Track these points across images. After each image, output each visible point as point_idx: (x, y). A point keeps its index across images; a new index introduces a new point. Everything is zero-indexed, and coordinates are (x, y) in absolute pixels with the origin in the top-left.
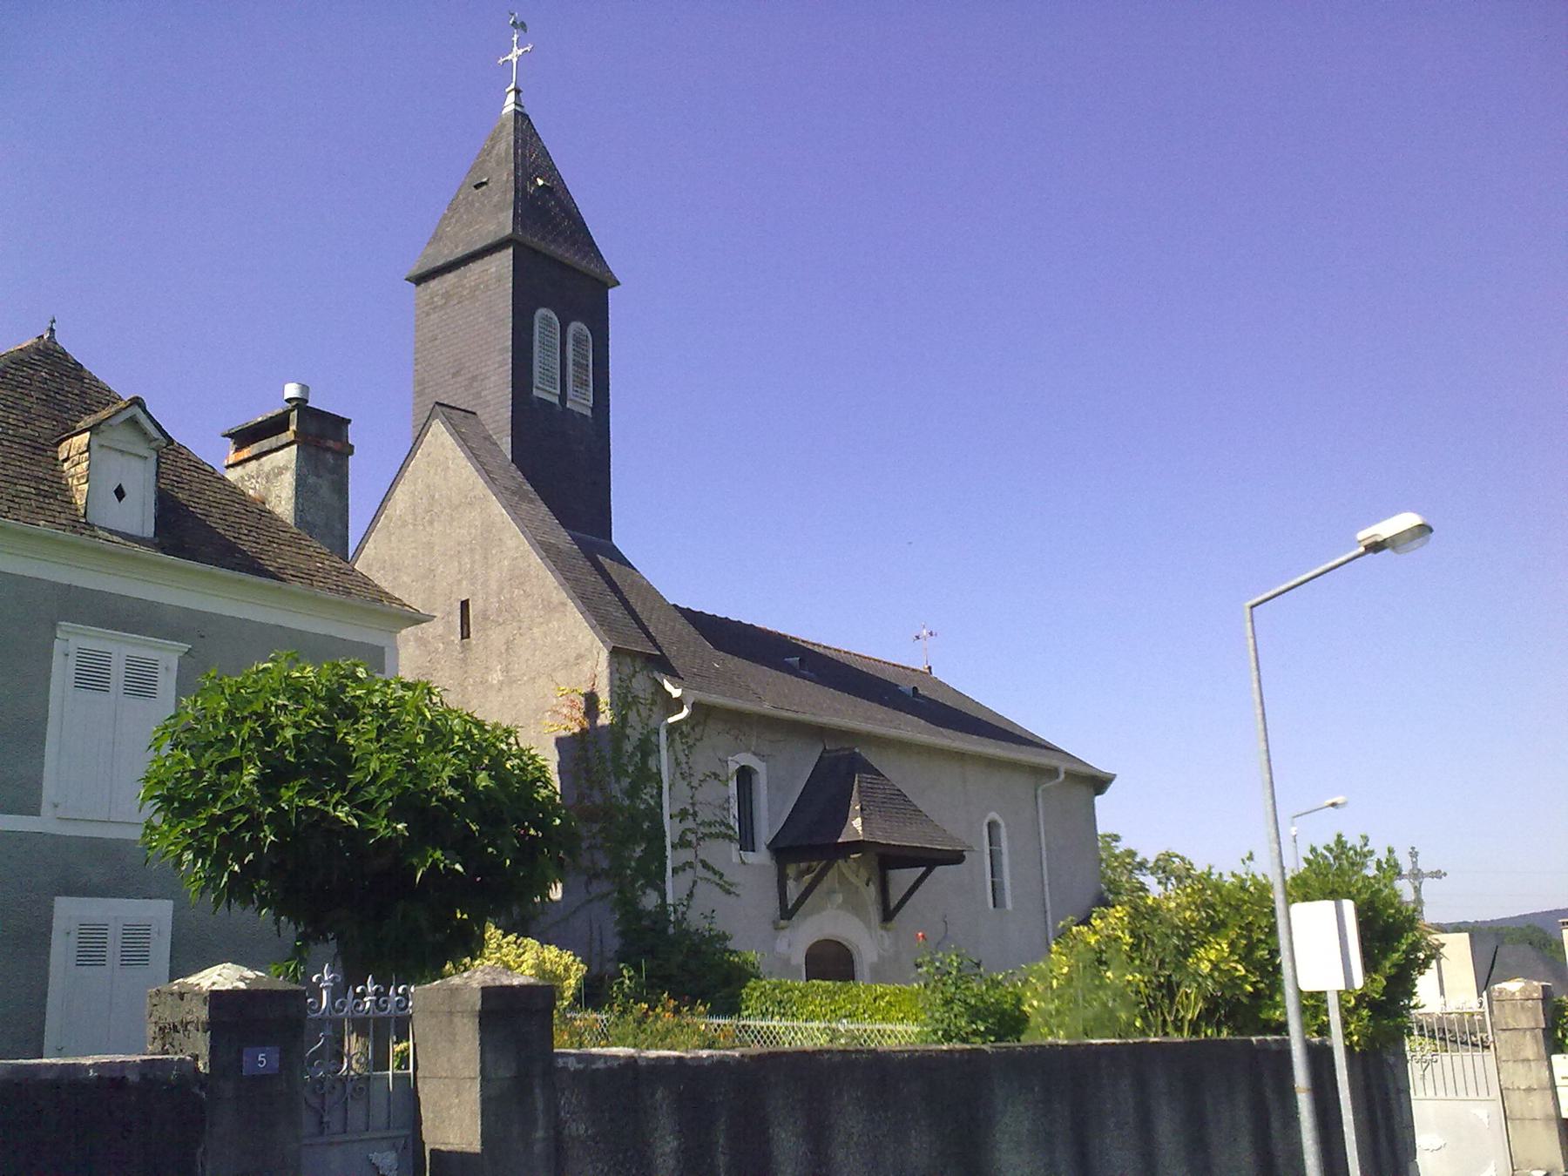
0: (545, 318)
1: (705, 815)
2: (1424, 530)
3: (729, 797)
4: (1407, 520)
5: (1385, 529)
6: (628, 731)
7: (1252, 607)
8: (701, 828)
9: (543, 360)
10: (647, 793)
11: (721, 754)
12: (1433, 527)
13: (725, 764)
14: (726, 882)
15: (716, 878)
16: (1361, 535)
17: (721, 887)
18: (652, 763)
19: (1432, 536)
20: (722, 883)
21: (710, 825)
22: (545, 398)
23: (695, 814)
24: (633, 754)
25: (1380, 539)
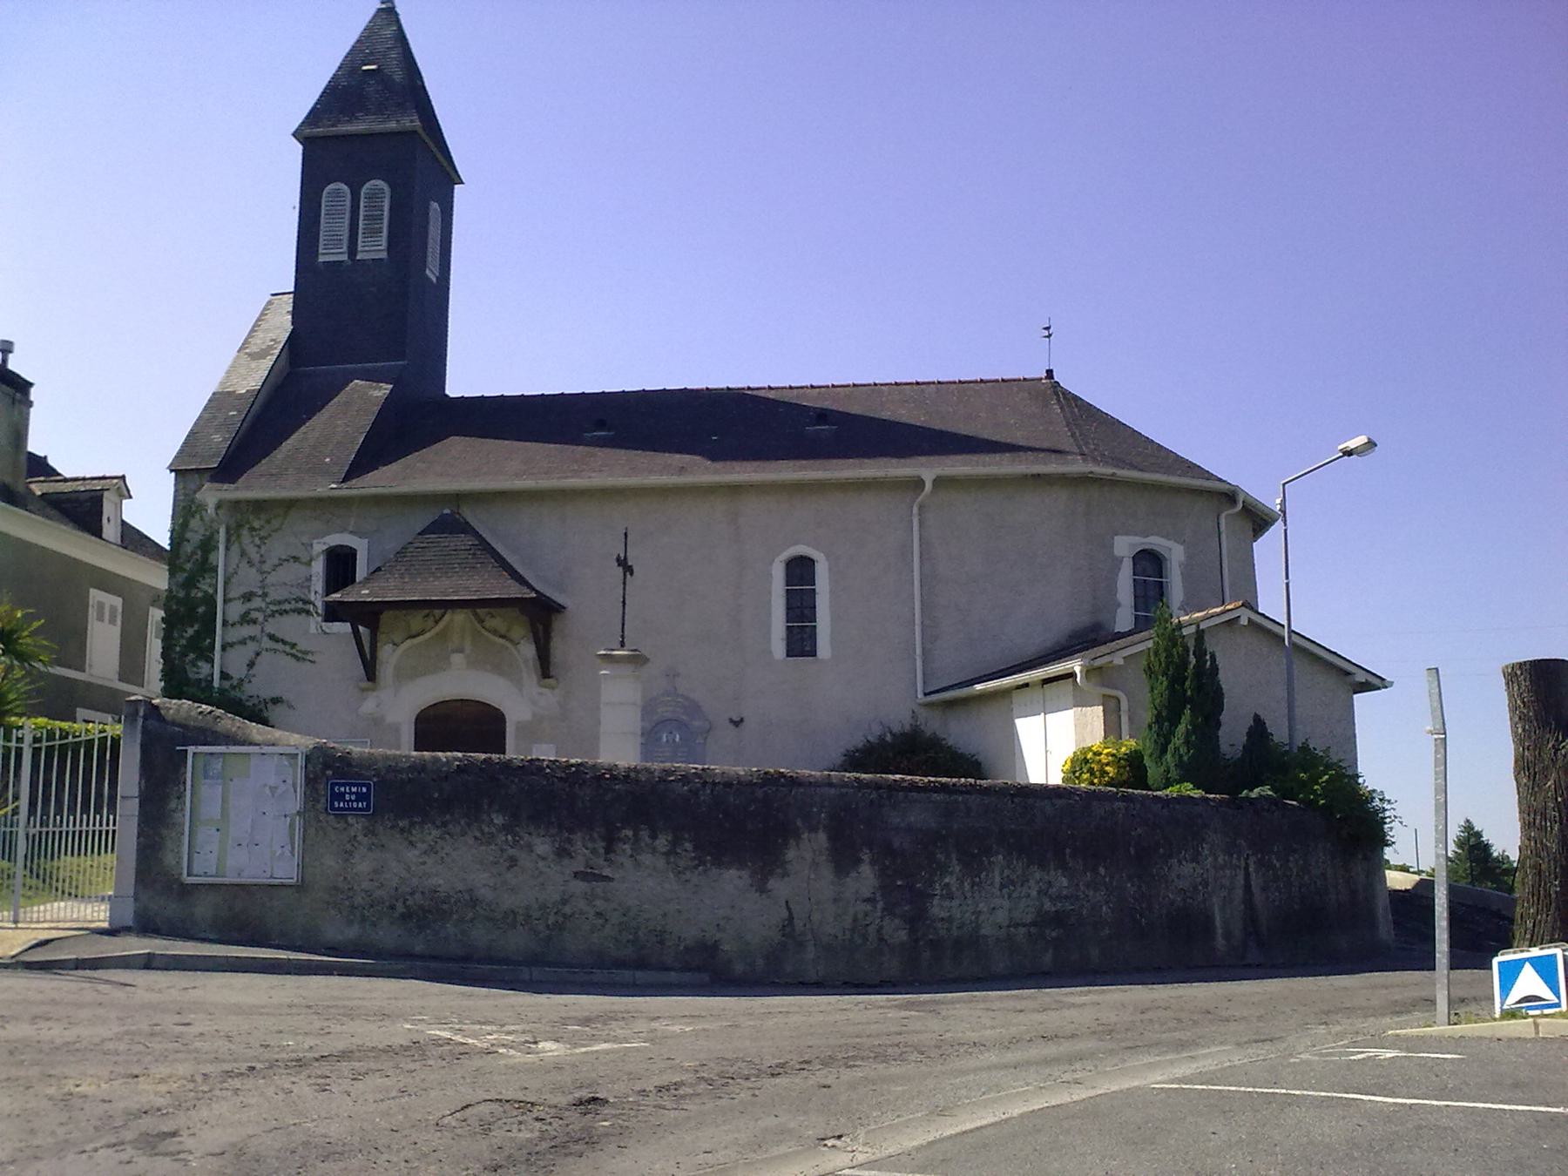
0: (337, 193)
1: (274, 595)
2: (1371, 444)
3: (311, 576)
4: (1362, 440)
5: (1352, 444)
6: (188, 535)
7: (1284, 485)
8: (271, 606)
9: (333, 227)
10: (205, 585)
11: (305, 539)
12: (1377, 443)
13: (309, 548)
14: (301, 651)
15: (287, 649)
16: (1341, 447)
17: (293, 655)
18: (212, 557)
19: (1376, 448)
20: (294, 651)
21: (280, 603)
22: (327, 260)
23: (265, 595)
24: (194, 553)
25: (1349, 449)
